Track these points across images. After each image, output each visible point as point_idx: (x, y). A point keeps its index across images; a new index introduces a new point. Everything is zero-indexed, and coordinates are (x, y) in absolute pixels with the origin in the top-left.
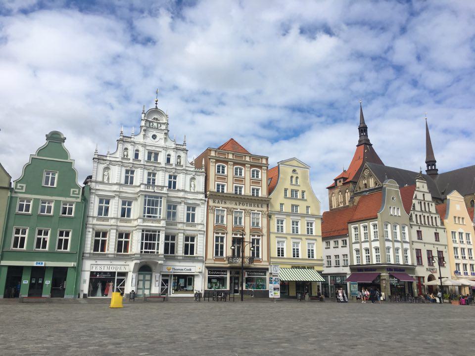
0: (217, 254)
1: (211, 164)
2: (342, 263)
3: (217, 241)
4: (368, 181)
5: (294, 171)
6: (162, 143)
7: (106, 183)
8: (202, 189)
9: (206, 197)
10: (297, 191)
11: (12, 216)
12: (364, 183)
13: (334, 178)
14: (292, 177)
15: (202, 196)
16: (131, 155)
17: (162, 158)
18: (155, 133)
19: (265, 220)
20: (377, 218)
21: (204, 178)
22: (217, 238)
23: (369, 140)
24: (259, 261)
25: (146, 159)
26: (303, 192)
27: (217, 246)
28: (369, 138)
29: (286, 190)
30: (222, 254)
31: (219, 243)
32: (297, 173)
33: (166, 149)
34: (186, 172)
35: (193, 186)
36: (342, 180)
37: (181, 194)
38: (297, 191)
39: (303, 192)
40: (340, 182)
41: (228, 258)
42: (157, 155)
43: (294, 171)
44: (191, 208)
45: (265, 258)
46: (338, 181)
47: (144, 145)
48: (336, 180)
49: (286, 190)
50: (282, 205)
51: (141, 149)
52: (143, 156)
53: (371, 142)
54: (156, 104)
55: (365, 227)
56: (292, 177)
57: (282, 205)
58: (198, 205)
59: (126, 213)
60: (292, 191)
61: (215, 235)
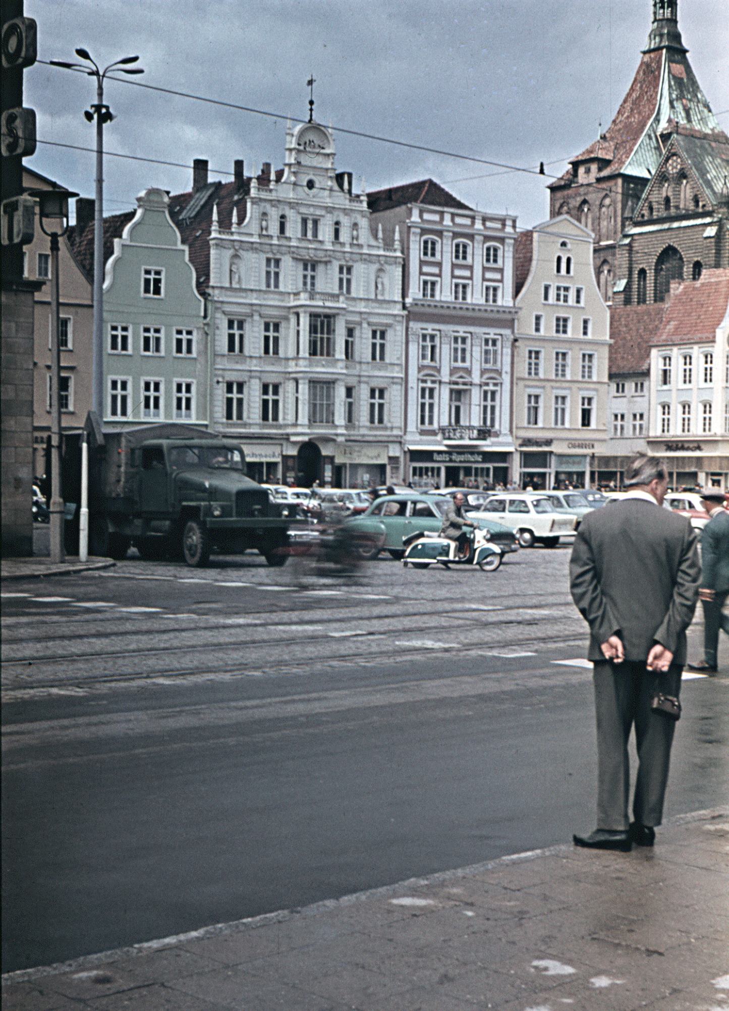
0: (423, 422)
1: (412, 238)
2: (628, 432)
3: (423, 397)
4: (677, 194)
5: (564, 244)
6: (327, 200)
7: (236, 289)
8: (398, 298)
9: (404, 307)
10: (566, 289)
11: (105, 357)
12: (664, 195)
13: (573, 159)
14: (559, 259)
15: (397, 310)
16: (274, 229)
17: (326, 233)
18: (311, 177)
19: (507, 351)
20: (714, 342)
21: (400, 269)
22: (423, 390)
23: (676, 37)
24: (497, 435)
25: (299, 236)
26: (579, 291)
27: (423, 405)
28: (680, 27)
29: (547, 288)
30: (431, 422)
31: (427, 401)
32: (569, 250)
33: (330, 210)
34: (368, 259)
35: (380, 286)
36: (594, 167)
37: (361, 307)
38: (566, 289)
39: (579, 291)
40: (588, 171)
41: (442, 430)
42: (316, 222)
43: (564, 244)
44: (380, 333)
45: (505, 429)
46: (581, 170)
47: (292, 205)
48: (576, 165)
49: (547, 288)
50: (538, 318)
51: (291, 214)
52: (293, 229)
53: (685, 43)
54: (311, 110)
55: (688, 359)
56: (559, 259)
57: (538, 318)
58: (389, 326)
59: (271, 346)
60: (558, 288)
61: (421, 385)
